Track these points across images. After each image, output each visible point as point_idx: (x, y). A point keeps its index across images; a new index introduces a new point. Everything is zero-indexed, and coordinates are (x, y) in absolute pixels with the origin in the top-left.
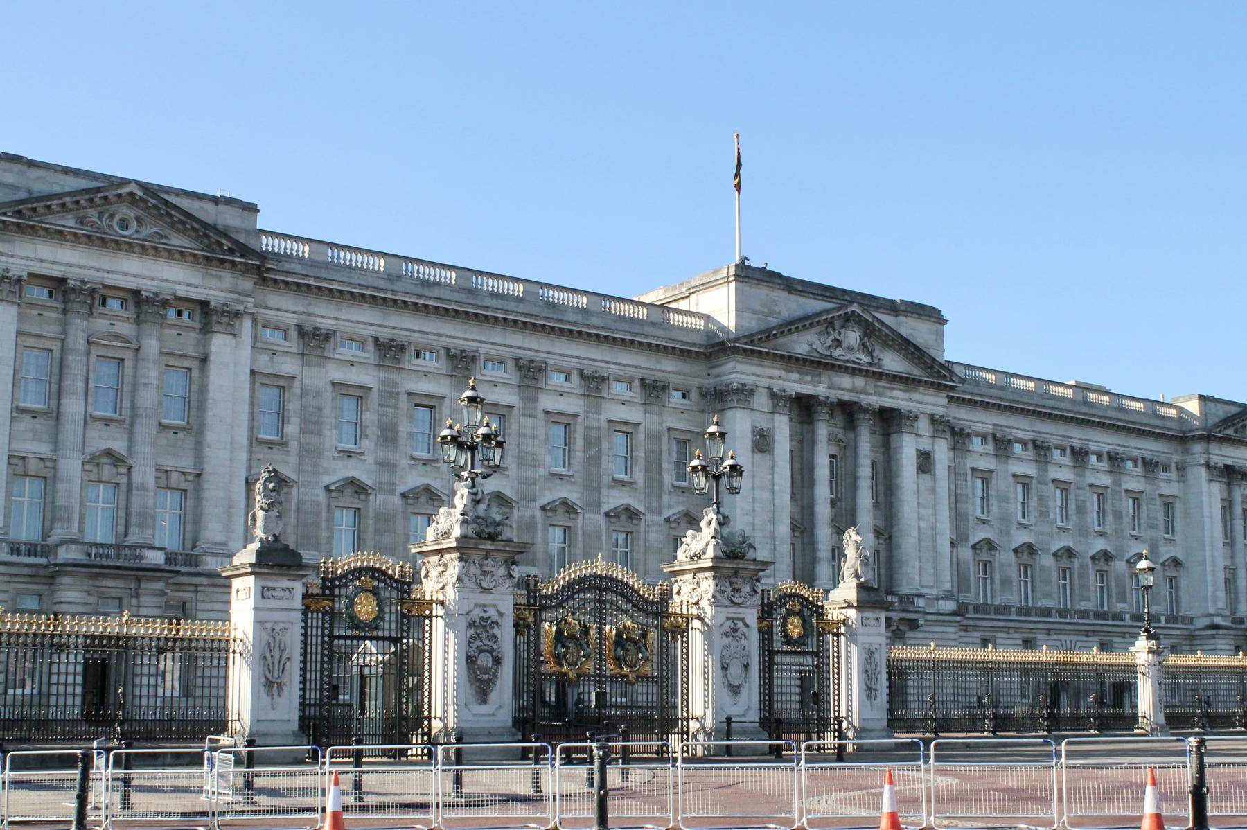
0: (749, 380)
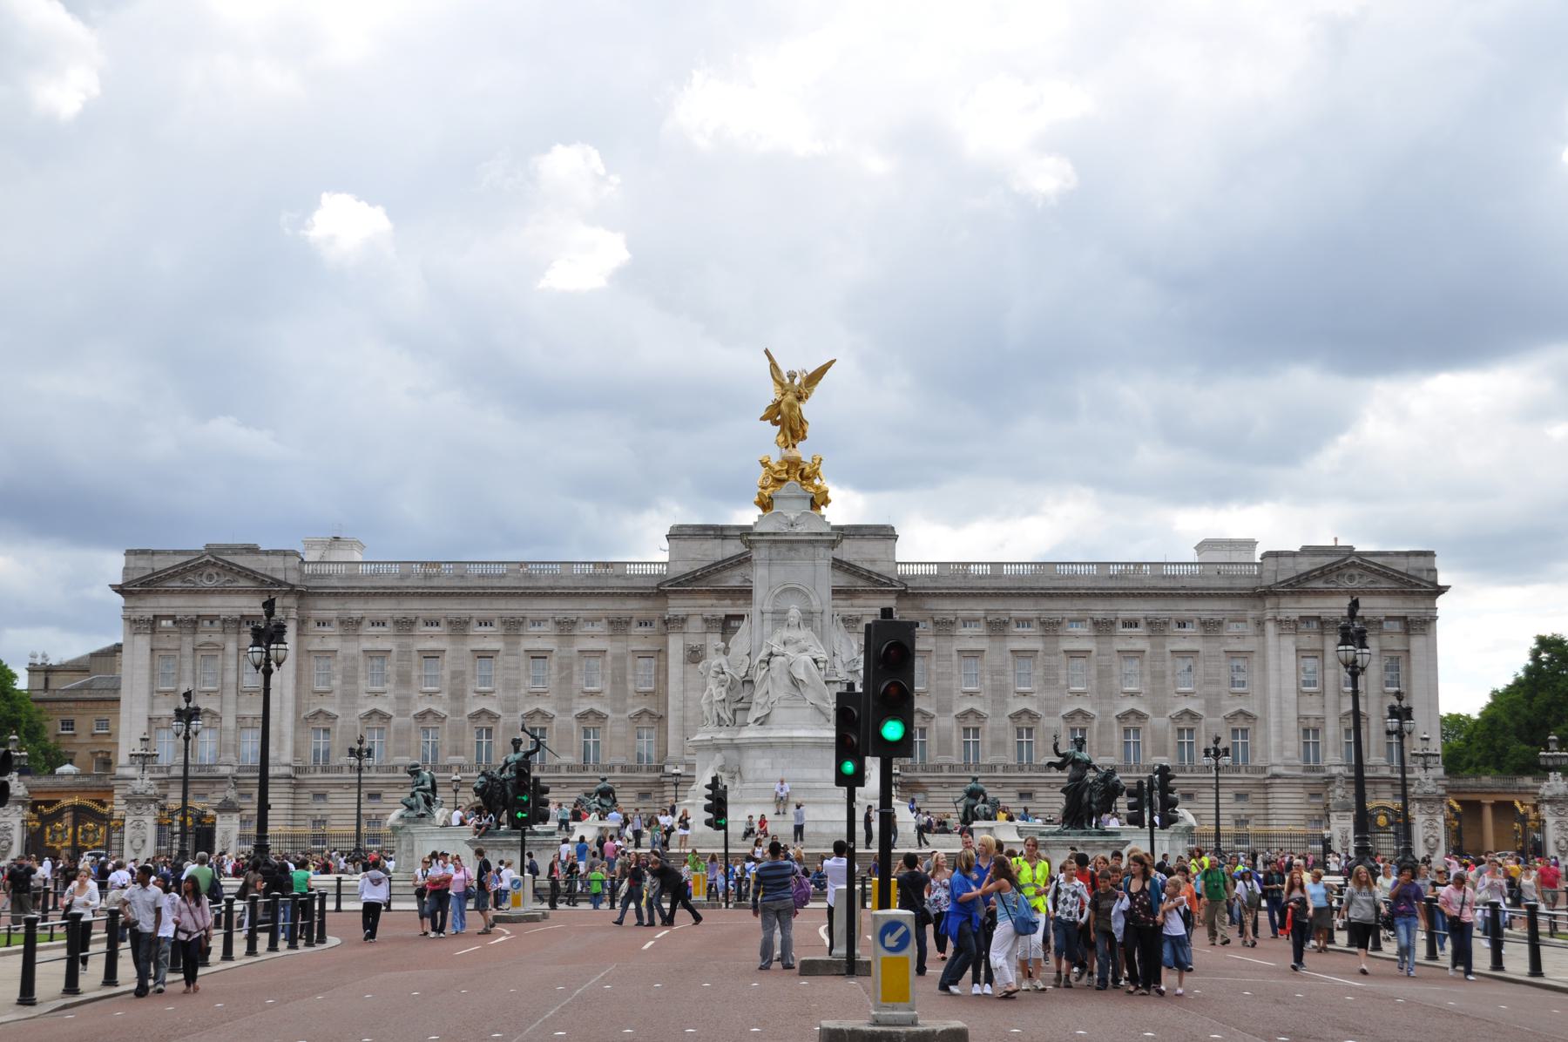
0: (681, 612)
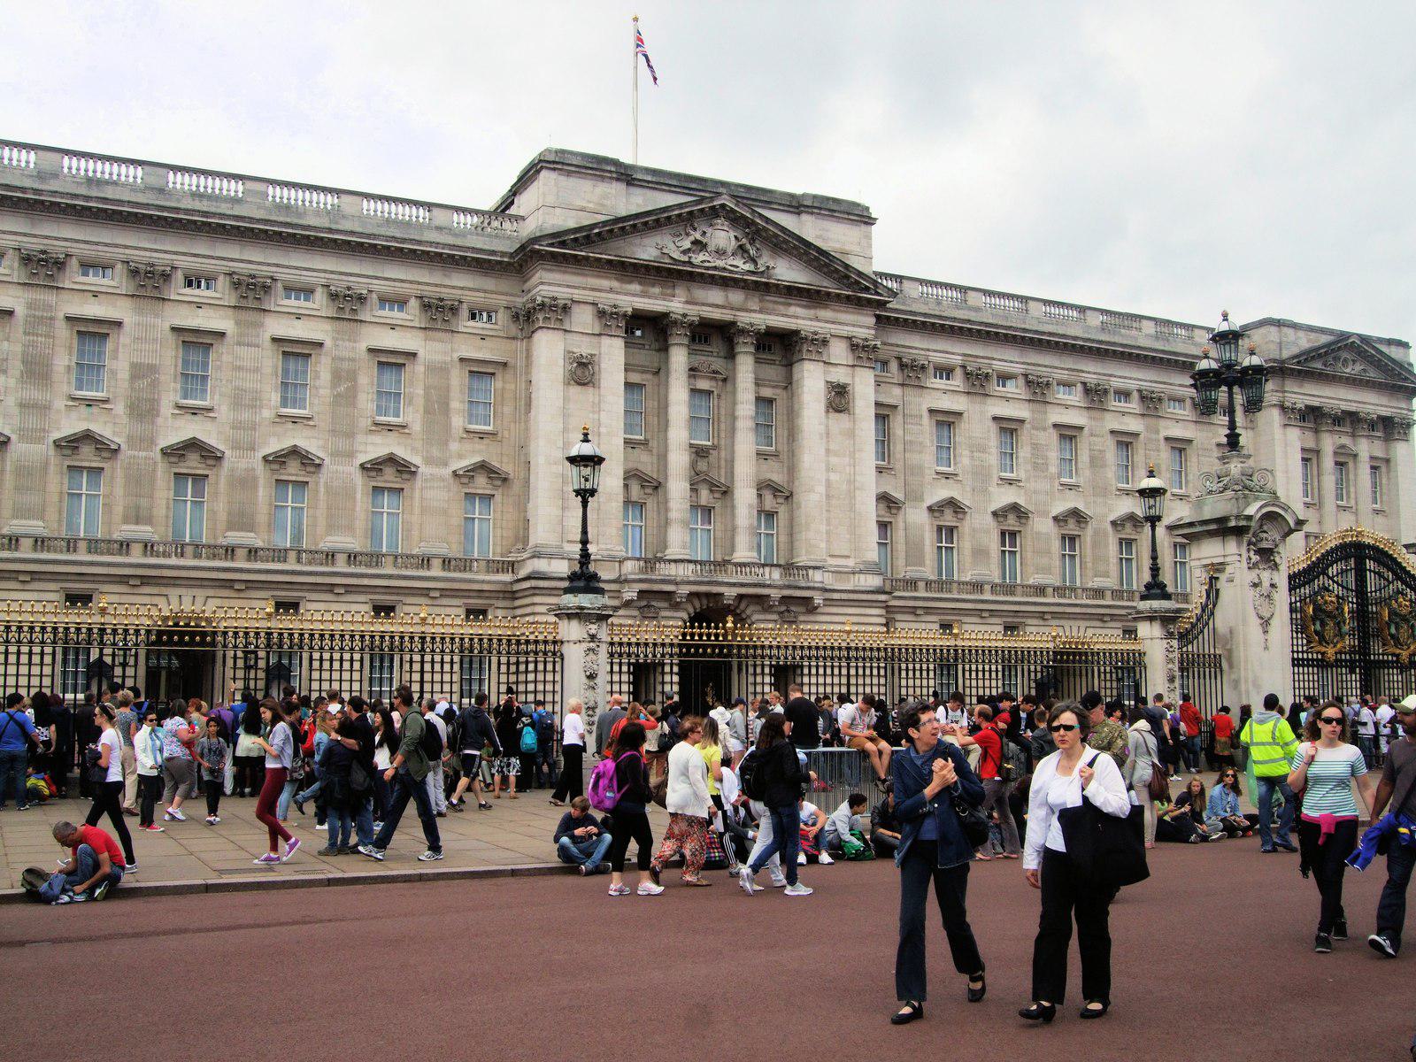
0: (563, 293)
